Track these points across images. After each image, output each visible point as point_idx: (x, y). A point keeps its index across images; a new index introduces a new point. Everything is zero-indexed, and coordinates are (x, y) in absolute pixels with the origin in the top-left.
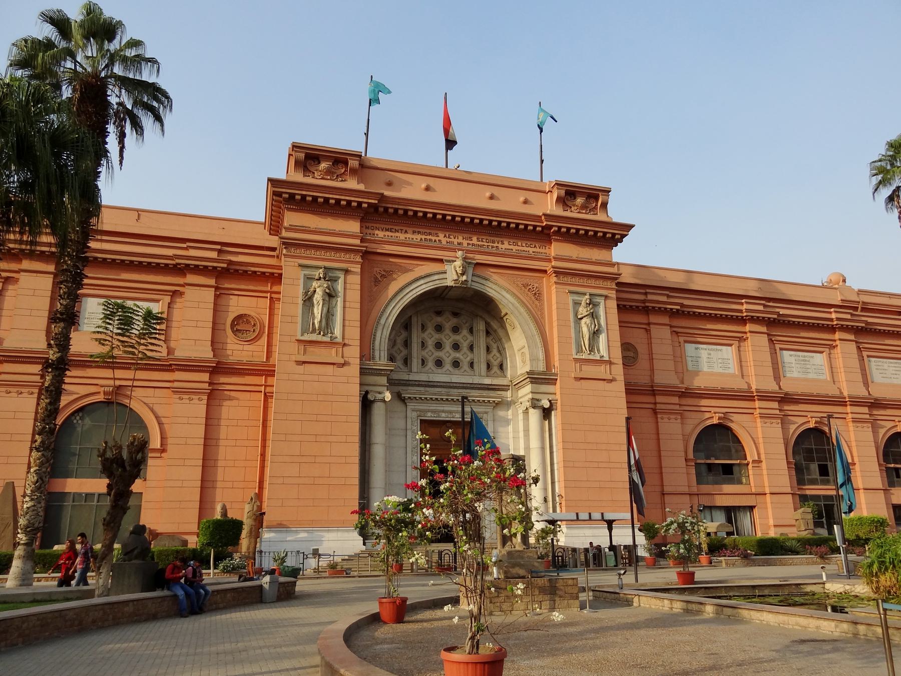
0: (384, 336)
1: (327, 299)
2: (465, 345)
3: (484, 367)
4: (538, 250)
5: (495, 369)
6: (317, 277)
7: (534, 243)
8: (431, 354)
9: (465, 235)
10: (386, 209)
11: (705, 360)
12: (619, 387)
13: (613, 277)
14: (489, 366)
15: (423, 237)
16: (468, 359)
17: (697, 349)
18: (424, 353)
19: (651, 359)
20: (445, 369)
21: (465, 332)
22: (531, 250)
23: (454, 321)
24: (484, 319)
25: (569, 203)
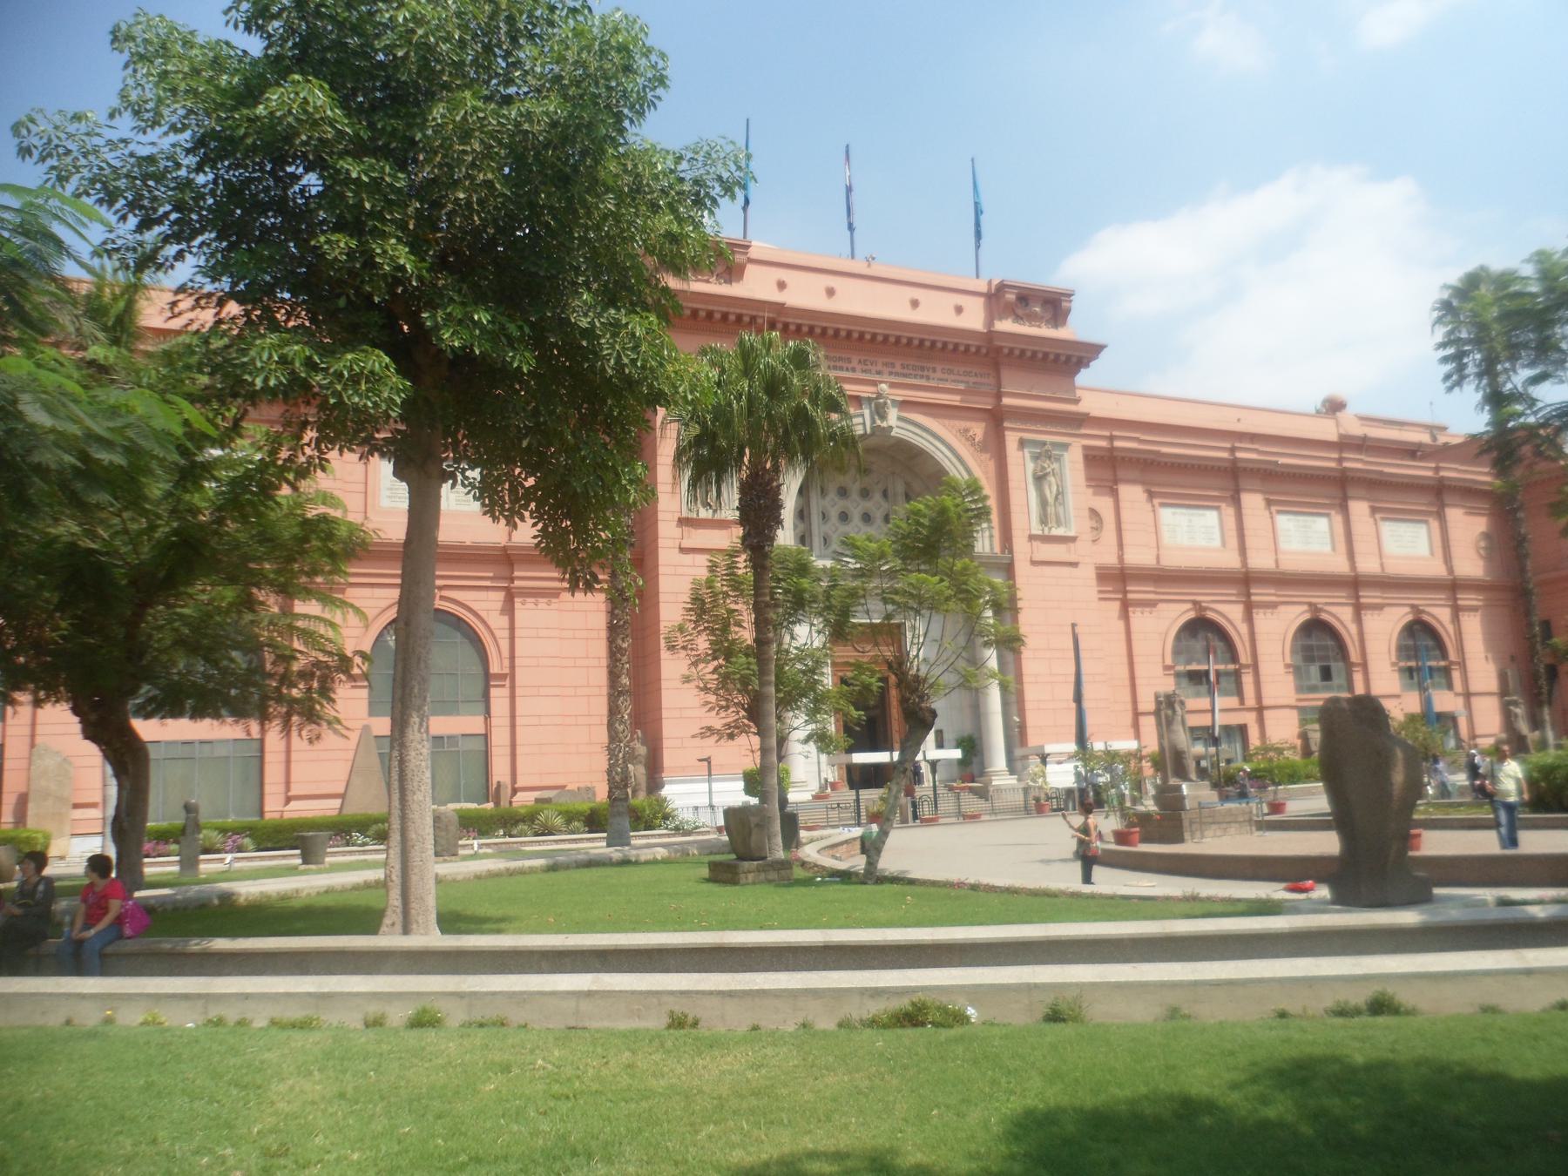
2: (878, 515)
4: (979, 379)
12: (1087, 573)
13: (1079, 421)
25: (1020, 312)
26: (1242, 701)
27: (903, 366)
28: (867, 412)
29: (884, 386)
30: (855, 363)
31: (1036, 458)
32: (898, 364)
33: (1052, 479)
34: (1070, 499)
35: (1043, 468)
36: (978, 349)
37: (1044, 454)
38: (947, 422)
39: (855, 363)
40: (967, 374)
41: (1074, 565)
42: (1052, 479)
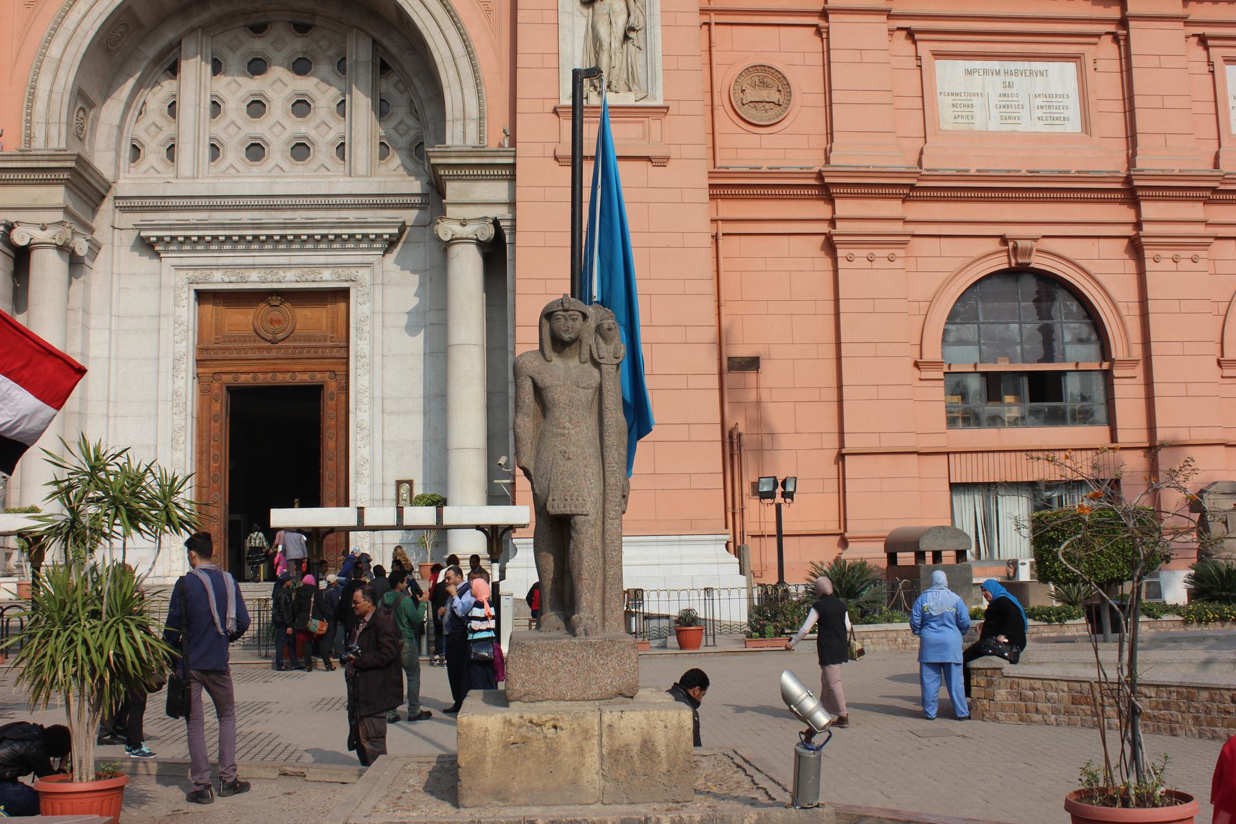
0: (58, 88)
3: (362, 151)
8: (236, 128)
11: (995, 100)
14: (384, 149)
16: (332, 136)
17: (969, 72)
18: (219, 129)
19: (829, 105)
23: (297, 45)
24: (368, 34)
26: (1114, 438)
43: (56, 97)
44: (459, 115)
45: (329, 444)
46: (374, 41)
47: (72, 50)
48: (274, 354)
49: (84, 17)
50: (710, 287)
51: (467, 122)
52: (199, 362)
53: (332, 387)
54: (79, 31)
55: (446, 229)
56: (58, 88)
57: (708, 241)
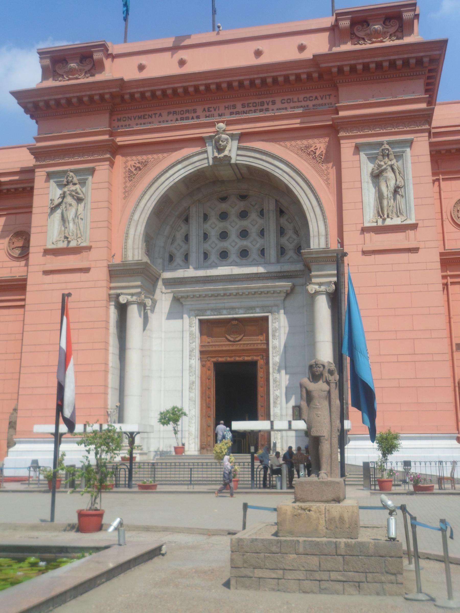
0: (138, 233)
1: (74, 203)
2: (254, 231)
3: (272, 253)
4: (320, 101)
5: (291, 254)
6: (65, 182)
7: (314, 95)
8: (215, 245)
9: (227, 104)
10: (132, 95)
12: (430, 258)
14: (282, 251)
15: (179, 117)
16: (258, 245)
18: (207, 246)
20: (230, 260)
21: (254, 216)
22: (310, 104)
23: (241, 205)
25: (361, 34)
27: (243, 106)
28: (209, 149)
29: (221, 125)
30: (200, 111)
31: (372, 159)
32: (239, 105)
33: (390, 174)
34: (411, 190)
35: (380, 166)
36: (309, 75)
37: (379, 153)
38: (288, 143)
39: (200, 111)
40: (305, 99)
41: (415, 250)
42: (390, 174)
43: (137, 237)
44: (316, 234)
45: (261, 390)
46: (276, 200)
47: (143, 216)
48: (234, 348)
49: (148, 201)
50: (444, 310)
51: (320, 237)
52: (202, 352)
53: (261, 363)
54: (146, 208)
55: (312, 288)
56: (138, 233)
57: (441, 287)
